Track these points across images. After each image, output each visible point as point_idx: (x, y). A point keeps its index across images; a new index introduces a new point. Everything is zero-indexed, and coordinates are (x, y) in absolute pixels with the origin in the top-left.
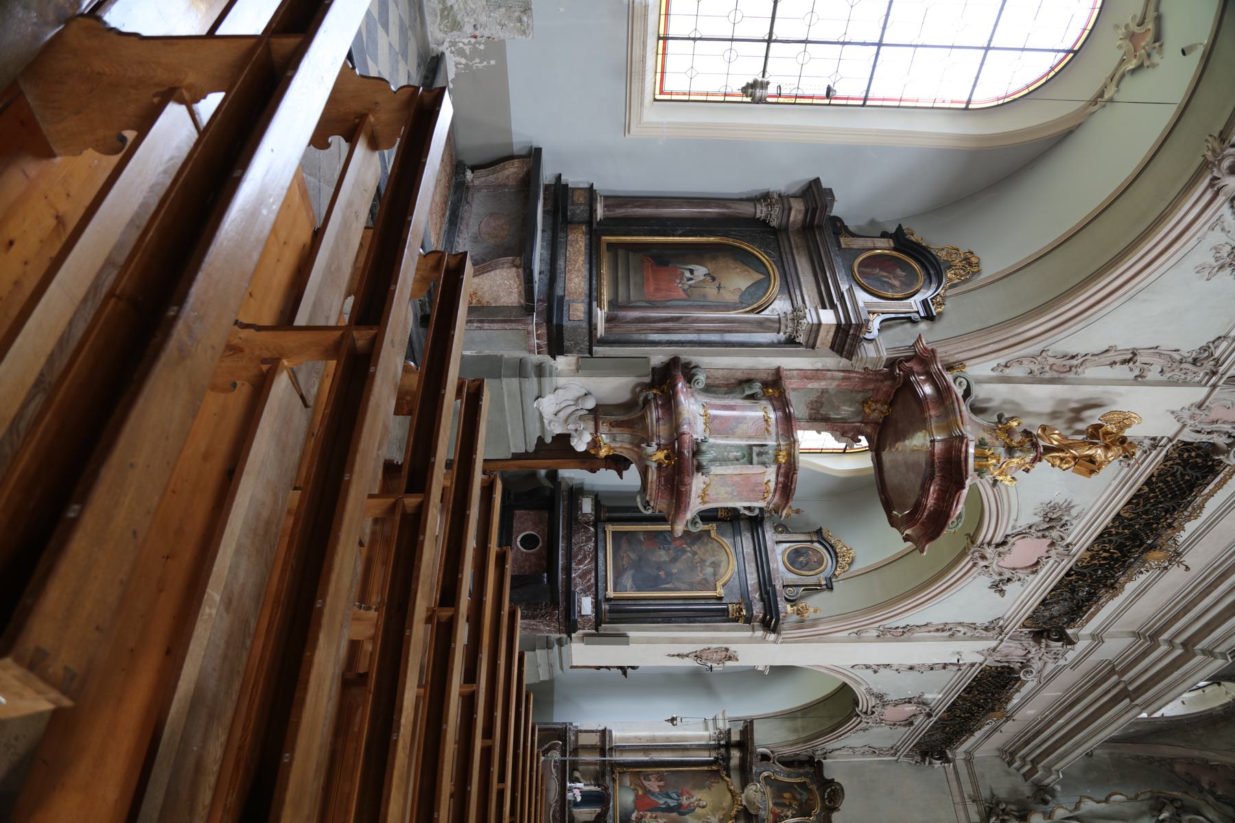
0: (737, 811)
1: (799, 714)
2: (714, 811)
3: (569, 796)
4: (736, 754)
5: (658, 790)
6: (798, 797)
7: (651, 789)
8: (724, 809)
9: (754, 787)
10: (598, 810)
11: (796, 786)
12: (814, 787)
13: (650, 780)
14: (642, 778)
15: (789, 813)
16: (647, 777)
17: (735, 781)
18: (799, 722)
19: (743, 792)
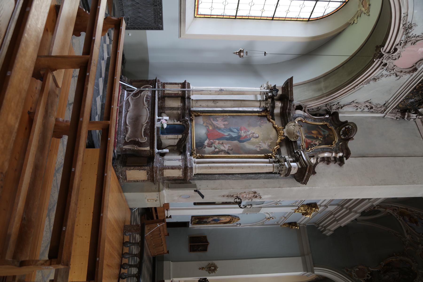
0: (281, 140)
1: (322, 79)
2: (264, 140)
3: (157, 125)
4: (278, 104)
5: (223, 127)
6: (322, 133)
7: (218, 126)
8: (271, 139)
9: (293, 124)
10: (180, 136)
11: (320, 127)
12: (333, 128)
13: (218, 121)
14: (212, 120)
15: (317, 143)
16: (215, 119)
17: (277, 123)
18: (322, 85)
19: (285, 128)
